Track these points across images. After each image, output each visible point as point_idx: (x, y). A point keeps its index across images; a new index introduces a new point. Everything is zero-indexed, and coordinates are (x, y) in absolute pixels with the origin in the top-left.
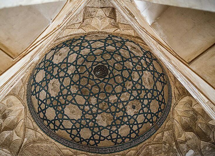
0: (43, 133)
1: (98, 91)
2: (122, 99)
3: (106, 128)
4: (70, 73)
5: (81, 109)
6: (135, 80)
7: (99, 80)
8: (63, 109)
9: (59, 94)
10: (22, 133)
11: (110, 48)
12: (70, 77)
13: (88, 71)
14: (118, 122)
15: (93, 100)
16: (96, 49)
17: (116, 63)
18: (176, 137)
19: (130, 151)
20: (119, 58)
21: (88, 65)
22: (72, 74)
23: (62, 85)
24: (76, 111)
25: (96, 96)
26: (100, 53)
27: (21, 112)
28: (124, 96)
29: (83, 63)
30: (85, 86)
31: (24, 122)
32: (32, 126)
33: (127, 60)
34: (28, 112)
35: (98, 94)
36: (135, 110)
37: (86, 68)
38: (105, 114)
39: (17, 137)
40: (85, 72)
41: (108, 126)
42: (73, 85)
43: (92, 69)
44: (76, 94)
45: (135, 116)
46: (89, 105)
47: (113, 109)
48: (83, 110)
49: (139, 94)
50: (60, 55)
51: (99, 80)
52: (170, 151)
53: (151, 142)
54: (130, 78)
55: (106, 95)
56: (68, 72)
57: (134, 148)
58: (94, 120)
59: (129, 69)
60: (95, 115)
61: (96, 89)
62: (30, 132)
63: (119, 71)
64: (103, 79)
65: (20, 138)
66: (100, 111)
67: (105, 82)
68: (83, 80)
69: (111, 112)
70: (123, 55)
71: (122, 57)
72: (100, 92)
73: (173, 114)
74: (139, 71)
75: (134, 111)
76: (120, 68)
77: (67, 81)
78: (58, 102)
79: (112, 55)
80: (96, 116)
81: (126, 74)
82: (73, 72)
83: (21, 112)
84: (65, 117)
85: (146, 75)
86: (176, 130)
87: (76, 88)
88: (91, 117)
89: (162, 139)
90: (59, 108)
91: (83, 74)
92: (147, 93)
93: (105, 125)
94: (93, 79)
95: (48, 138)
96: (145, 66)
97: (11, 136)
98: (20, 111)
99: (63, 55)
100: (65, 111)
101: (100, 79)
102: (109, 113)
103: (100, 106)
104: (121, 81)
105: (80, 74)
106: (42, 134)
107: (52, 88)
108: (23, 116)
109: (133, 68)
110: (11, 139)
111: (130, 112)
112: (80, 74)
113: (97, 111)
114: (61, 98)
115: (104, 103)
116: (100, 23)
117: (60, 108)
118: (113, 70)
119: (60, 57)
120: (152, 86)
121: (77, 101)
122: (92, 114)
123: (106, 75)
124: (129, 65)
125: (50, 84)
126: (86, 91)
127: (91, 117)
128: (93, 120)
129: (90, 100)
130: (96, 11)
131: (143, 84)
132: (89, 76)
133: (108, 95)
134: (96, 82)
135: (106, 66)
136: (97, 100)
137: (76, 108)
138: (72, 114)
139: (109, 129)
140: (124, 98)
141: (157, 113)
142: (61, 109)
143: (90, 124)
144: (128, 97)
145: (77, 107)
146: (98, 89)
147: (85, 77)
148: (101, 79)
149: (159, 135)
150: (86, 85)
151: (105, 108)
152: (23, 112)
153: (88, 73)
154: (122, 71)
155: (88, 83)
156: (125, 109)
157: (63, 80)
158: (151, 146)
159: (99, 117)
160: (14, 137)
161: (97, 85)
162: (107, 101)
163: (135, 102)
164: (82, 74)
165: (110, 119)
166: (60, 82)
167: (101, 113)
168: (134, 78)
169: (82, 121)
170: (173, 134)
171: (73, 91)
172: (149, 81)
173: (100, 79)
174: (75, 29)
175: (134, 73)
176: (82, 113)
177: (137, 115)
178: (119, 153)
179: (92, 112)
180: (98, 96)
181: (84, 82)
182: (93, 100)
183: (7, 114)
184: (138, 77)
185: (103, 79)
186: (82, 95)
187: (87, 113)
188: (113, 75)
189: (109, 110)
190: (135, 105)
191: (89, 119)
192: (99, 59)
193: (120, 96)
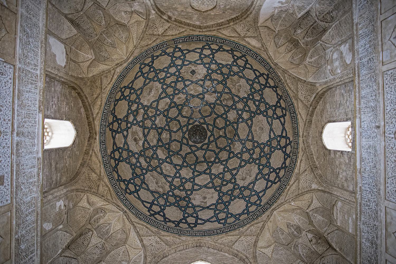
0: (299, 161)
1: (219, 118)
2: (201, 89)
3: (244, 77)
4: (222, 167)
5: (252, 121)
6: (168, 100)
7: (208, 128)
8: (264, 144)
9: (252, 162)
10: (307, 196)
11: (161, 154)
12: (227, 163)
13: (208, 147)
14: (225, 70)
15: (232, 116)
16: (175, 166)
17: (174, 132)
18: (144, 23)
19: (229, 37)
20: (165, 135)
21: (201, 154)
22: (222, 164)
23: (241, 166)
24: (258, 126)
25: (225, 116)
26: (178, 157)
27: (280, 211)
28: (196, 91)
29: (202, 162)
30: (225, 137)
31: (292, 201)
32: (295, 183)
33: (157, 128)
34: (279, 202)
35: (221, 116)
36: (193, 68)
37: (205, 153)
38: (233, 91)
39: (314, 201)
40: (211, 151)
41: (240, 77)
42: (233, 153)
43: (203, 145)
44: (240, 140)
45: (198, 62)
46: (240, 116)
47: (220, 88)
48: (251, 118)
49: (176, 83)
50: (205, 198)
51: (208, 128)
52: (166, 8)
53: (191, 30)
54: (173, 105)
55: (214, 107)
56: (222, 171)
57: (220, 35)
58: (251, 97)
59: (164, 116)
60: (245, 100)
61: (219, 123)
62: (303, 183)
63: (179, 121)
64: (203, 125)
65: (314, 197)
66: (237, 99)
67: (204, 120)
68: (221, 145)
69: (225, 86)
70: (157, 136)
71: (160, 134)
72: (218, 116)
73: (132, 53)
74: (154, 108)
75: (196, 68)
76: (174, 124)
77: (234, 163)
78: (261, 157)
79: (169, 144)
80: (245, 98)
81: (173, 113)
82: (218, 164)
83: (282, 211)
84: (272, 136)
85: (148, 100)
86: (141, 31)
87: (234, 146)
88: (250, 103)
89: (169, 28)
90: (267, 151)
91: (214, 151)
92: (164, 79)
93: (243, 81)
94: (212, 135)
95: (300, 150)
96: (142, 111)
97: (316, 210)
98: (282, 214)
99: (204, 195)
100: (266, 140)
101: (206, 128)
102: (228, 88)
103: (230, 103)
104: (186, 109)
105: (217, 154)
106: (301, 162)
107: (249, 176)
108: (286, 206)
109: (159, 115)
110: (321, 209)
111: (202, 71)
112: (217, 154)
113: (238, 102)
114: (254, 156)
115: (224, 102)
116: (114, 221)
117: (266, 149)
118: (184, 126)
119: (208, 196)
120: (150, 84)
121: (247, 134)
122: (246, 105)
123: (197, 125)
124: (160, 121)
125: (245, 184)
126: (230, 132)
127: (250, 103)
128: (251, 98)
129: (234, 119)
130: (95, 246)
131: (161, 90)
132: (213, 141)
133: (212, 106)
134: (213, 129)
135: (186, 136)
136: (229, 111)
137: (255, 128)
138: (264, 128)
139: (242, 73)
140: (197, 88)
141: (120, 99)
142: (266, 147)
143: (258, 98)
144: (191, 87)
145: (253, 127)
146: (218, 121)
147: (216, 144)
148: (205, 126)
149: (170, 33)
150: (224, 137)
151: (228, 97)
152: (282, 209)
153: (210, 146)
154: (175, 119)
155: (220, 136)
156: (206, 77)
157: (234, 169)
158: (195, 24)
159: (243, 94)
160: (316, 207)
161: (214, 126)
162: (219, 101)
163: (187, 76)
164: (215, 152)
165: (232, 81)
166: (238, 171)
167: (237, 96)
168: (167, 103)
169: (262, 110)
170: (146, 29)
171: (239, 147)
172: (150, 91)
173: (206, 128)
174: (126, 249)
175: (163, 108)
176: (254, 117)
177: (195, 62)
178: (246, 45)
179: (245, 107)
180: (224, 114)
181: (222, 143)
182: (232, 116)
183: (295, 227)
184: (162, 101)
185: (203, 125)
186: (236, 132)
187: (249, 111)
188: (189, 120)
189: (225, 91)
190: (190, 74)
191: (254, 103)
192: (186, 149)
193: (200, 94)
